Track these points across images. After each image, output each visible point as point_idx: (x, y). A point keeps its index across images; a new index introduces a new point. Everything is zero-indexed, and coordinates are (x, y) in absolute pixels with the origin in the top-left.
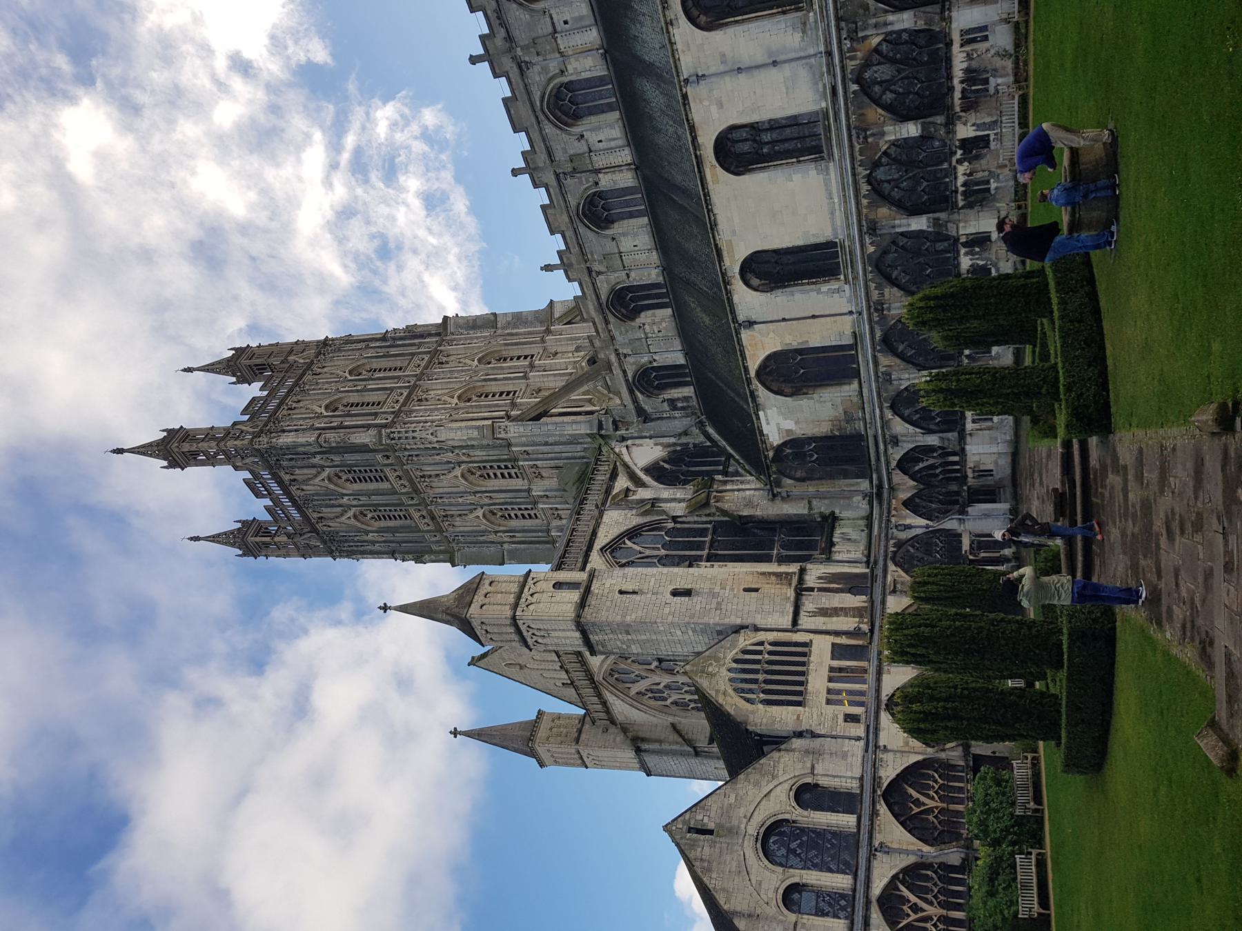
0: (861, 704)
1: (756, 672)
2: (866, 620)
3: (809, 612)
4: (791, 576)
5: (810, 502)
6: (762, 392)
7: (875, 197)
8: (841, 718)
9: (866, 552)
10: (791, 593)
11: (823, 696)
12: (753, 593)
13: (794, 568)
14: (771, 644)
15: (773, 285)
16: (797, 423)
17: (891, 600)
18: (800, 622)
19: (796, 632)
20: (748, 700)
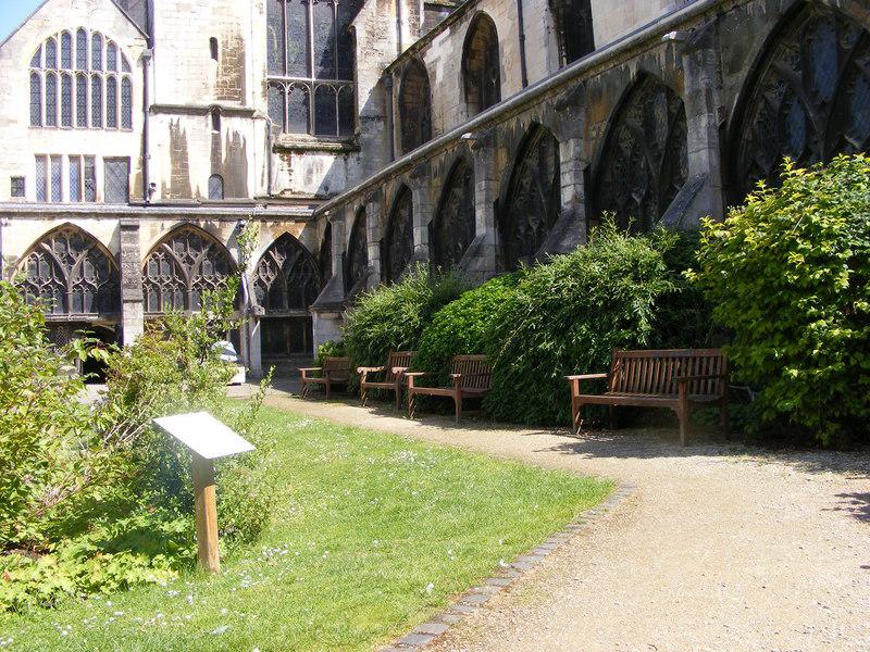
0: (42, 195)
1: (82, 60)
2: (168, 196)
3: (178, 125)
4: (237, 99)
5: (379, 118)
6: (464, 28)
7: (519, 138)
8: (17, 174)
9: (288, 195)
10: (209, 100)
11: (48, 151)
12: (208, 52)
13: (256, 100)
14: (126, 79)
15: (561, 11)
16: (441, 83)
17: (113, 224)
18: (161, 116)
19: (144, 110)
20: (36, 60)
